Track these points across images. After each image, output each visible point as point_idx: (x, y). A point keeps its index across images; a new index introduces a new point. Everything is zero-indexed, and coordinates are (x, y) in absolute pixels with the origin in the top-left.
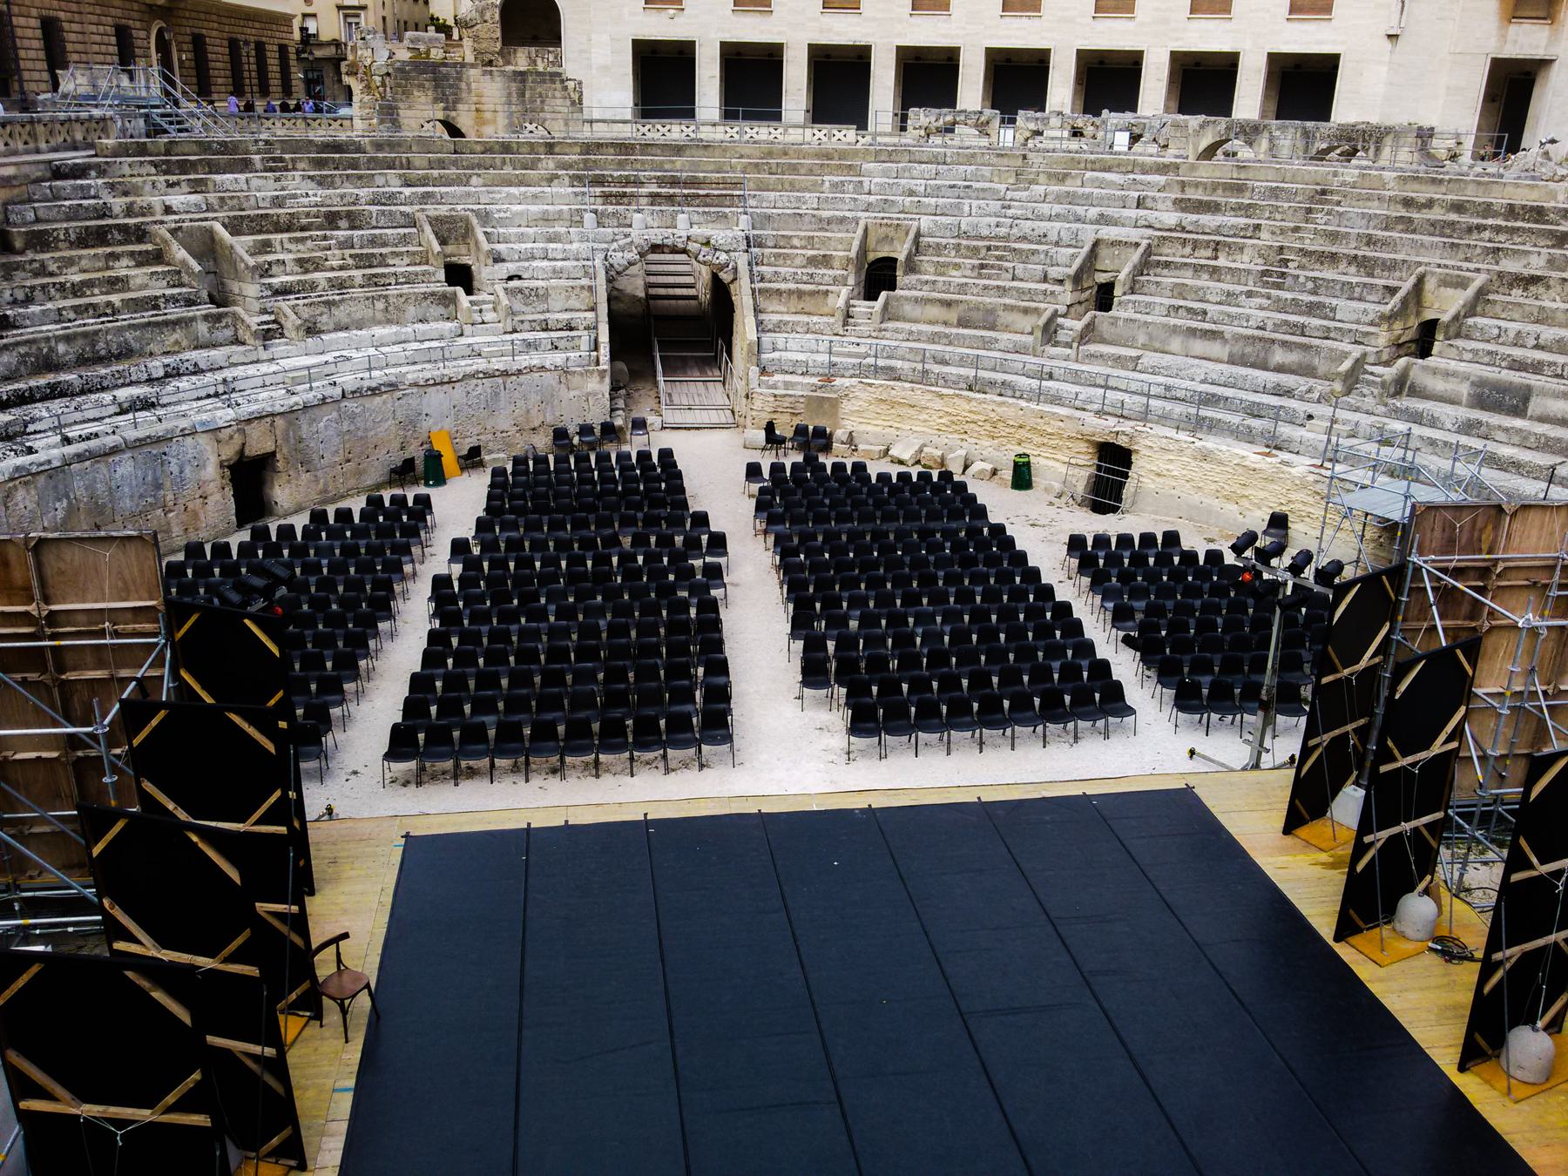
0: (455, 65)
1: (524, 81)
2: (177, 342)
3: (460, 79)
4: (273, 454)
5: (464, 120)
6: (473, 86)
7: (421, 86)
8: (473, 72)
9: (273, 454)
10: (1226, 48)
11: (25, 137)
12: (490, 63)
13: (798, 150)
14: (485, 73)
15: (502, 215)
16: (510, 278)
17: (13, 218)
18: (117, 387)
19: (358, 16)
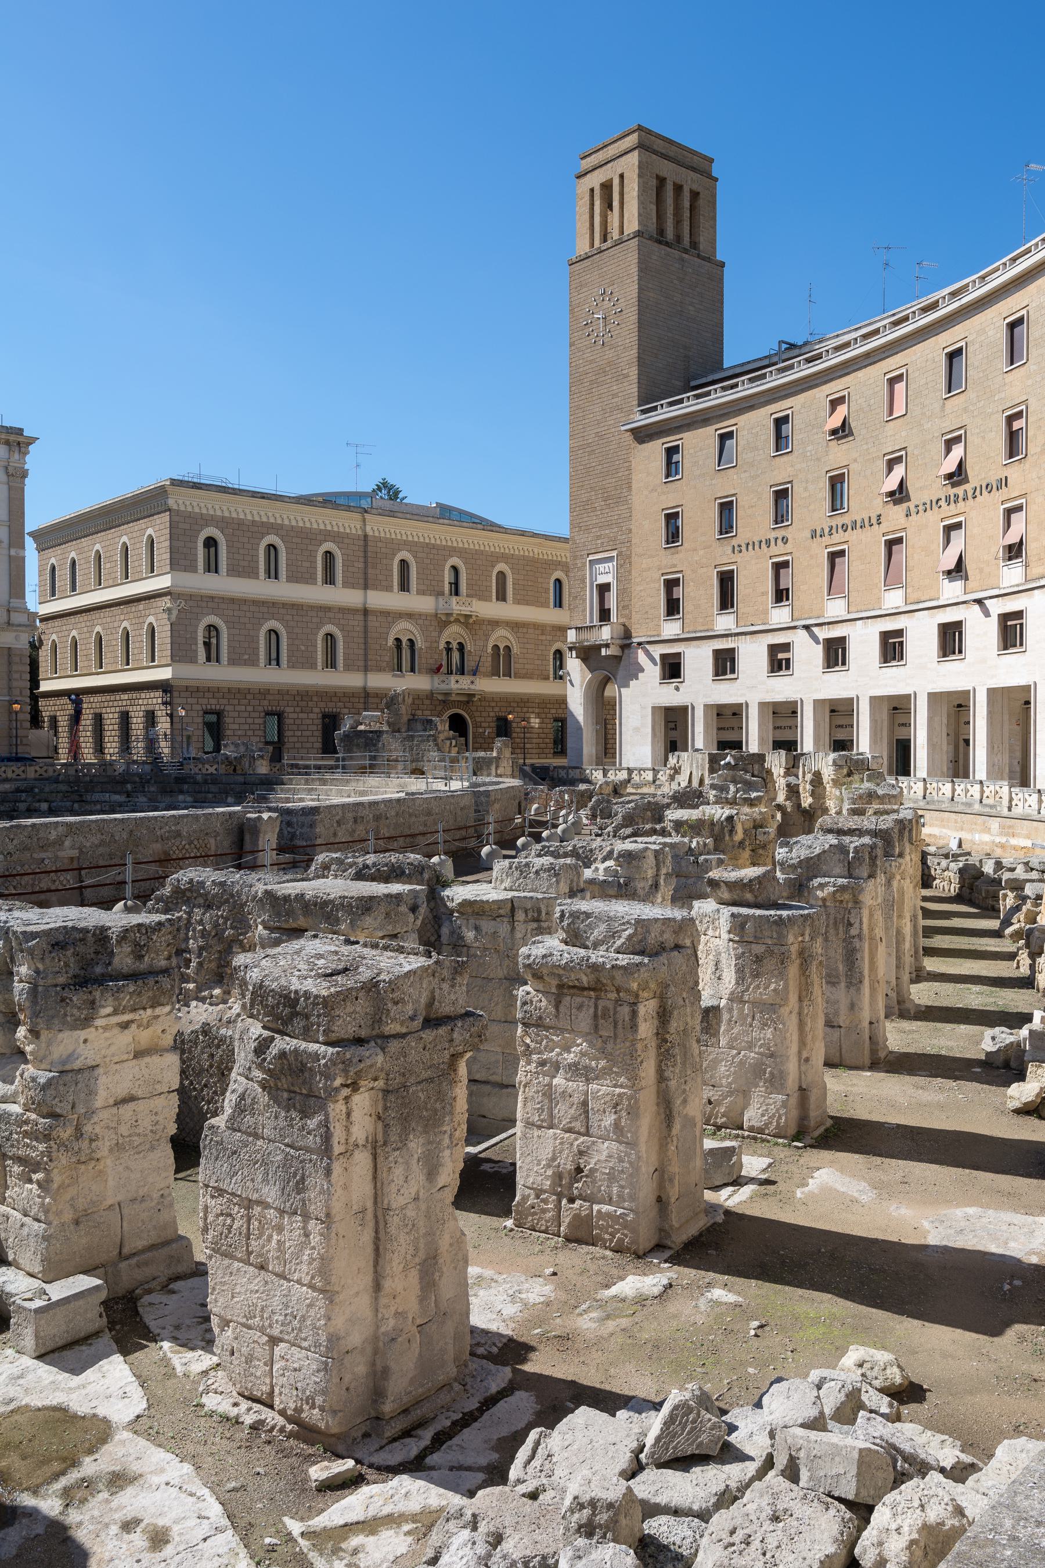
0: (376, 732)
10: (1023, 682)
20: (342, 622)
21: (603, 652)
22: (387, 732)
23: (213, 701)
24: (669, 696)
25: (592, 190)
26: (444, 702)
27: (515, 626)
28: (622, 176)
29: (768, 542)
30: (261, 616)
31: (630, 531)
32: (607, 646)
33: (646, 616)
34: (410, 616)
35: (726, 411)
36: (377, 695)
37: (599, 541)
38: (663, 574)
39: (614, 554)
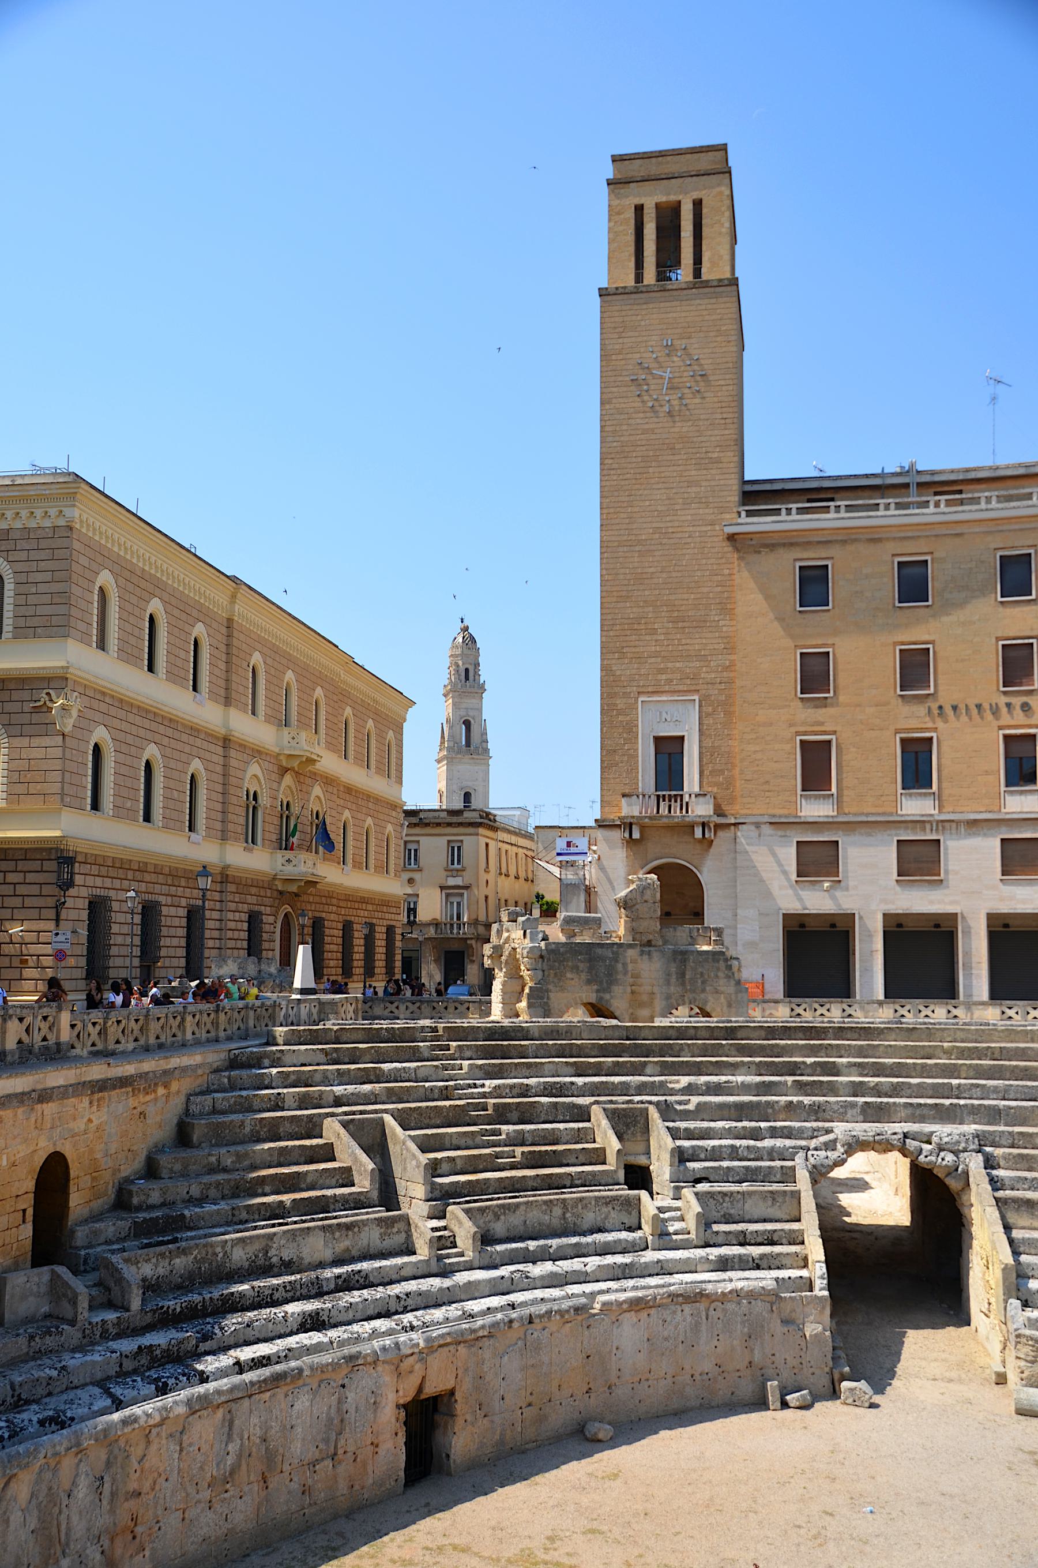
1: (684, 961)
2: (348, 1250)
3: (617, 961)
4: (452, 1393)
5: (618, 1001)
6: (630, 967)
7: (575, 969)
8: (630, 953)
9: (452, 1393)
11: (209, 1026)
12: (649, 943)
13: (986, 1032)
14: (642, 953)
15: (682, 1107)
16: (698, 1181)
17: (193, 1108)
18: (287, 1302)
19: (462, 895)
20: (208, 756)
21: (698, 833)
22: (630, 946)
23: (99, 882)
24: (817, 901)
25: (639, 209)
26: (281, 893)
27: (329, 781)
28: (698, 204)
29: (995, 712)
30: (142, 733)
31: (730, 667)
32: (704, 825)
33: (766, 787)
34: (257, 753)
35: (910, 534)
36: (237, 882)
37: (664, 677)
38: (798, 733)
39: (696, 697)
